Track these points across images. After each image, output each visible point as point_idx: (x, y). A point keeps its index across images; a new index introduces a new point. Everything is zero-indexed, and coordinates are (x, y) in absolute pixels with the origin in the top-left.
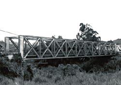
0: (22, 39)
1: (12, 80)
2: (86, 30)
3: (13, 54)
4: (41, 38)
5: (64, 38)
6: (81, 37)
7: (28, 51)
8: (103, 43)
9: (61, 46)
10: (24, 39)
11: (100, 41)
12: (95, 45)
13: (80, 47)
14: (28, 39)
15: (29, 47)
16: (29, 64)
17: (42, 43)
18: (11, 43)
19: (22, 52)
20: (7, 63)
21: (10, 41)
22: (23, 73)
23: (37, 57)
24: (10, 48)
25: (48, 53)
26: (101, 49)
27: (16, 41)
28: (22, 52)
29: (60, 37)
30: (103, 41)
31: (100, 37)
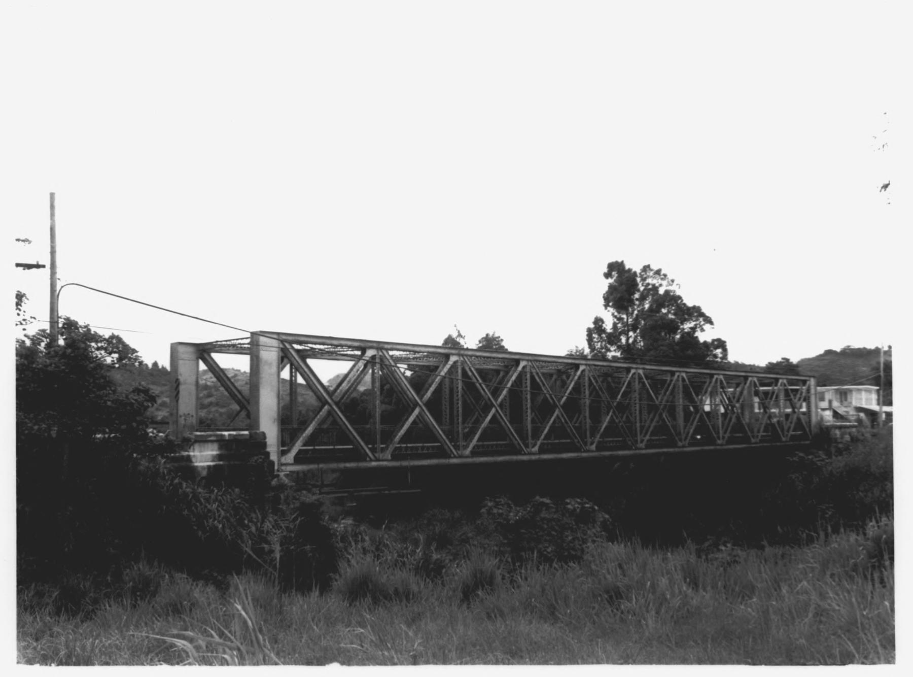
0: (270, 355)
1: (211, 589)
2: (643, 298)
3: (221, 441)
4: (380, 346)
5: (513, 345)
6: (613, 338)
7: (304, 424)
8: (743, 372)
9: (496, 392)
10: (285, 357)
11: (725, 366)
12: (696, 387)
13: (605, 396)
14: (304, 355)
15: (311, 399)
16: (309, 498)
17: (384, 380)
18: (210, 379)
19: (269, 427)
20: (186, 488)
21: (202, 366)
22: (277, 548)
23: (357, 454)
24: (201, 406)
25: (420, 432)
26: (730, 408)
27: (237, 364)
28: (269, 427)
29: (491, 344)
30: (738, 366)
31: (720, 344)
